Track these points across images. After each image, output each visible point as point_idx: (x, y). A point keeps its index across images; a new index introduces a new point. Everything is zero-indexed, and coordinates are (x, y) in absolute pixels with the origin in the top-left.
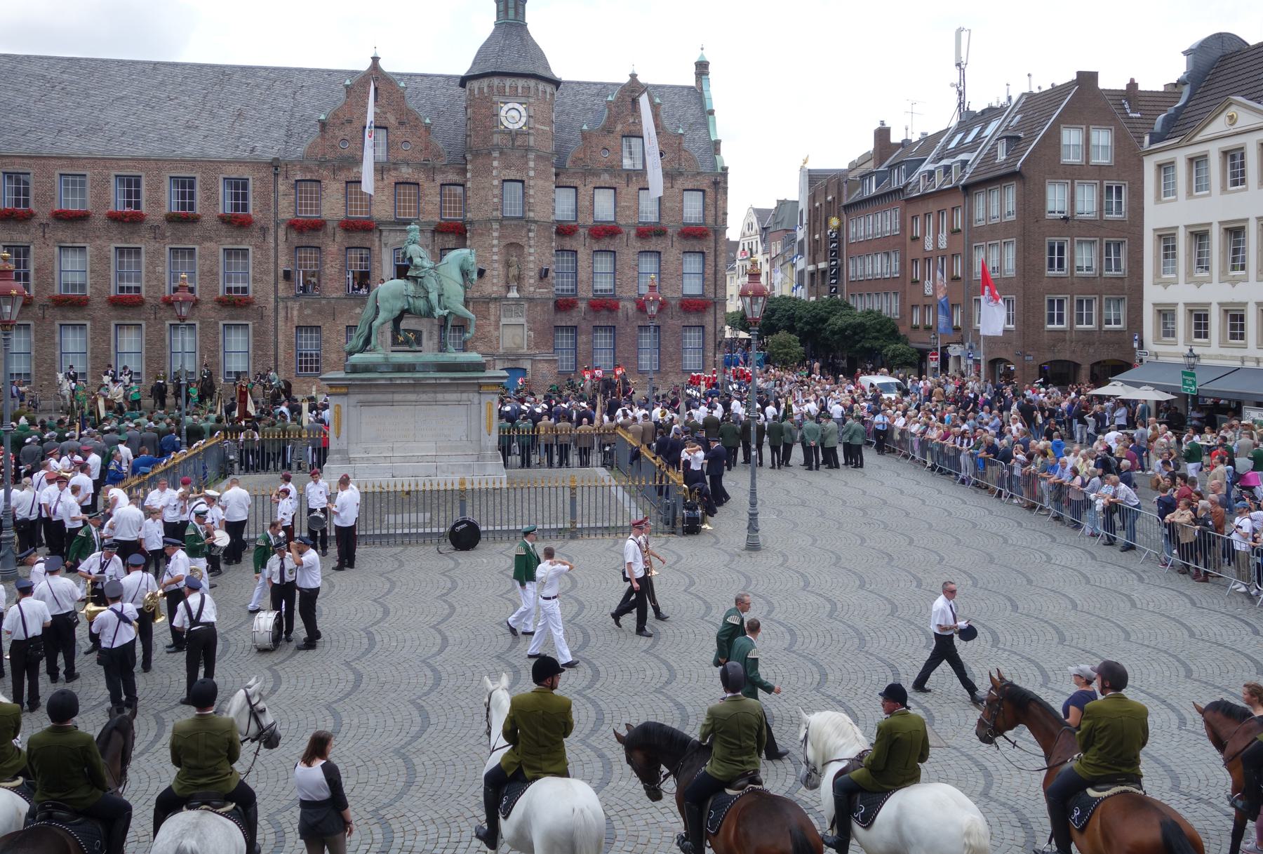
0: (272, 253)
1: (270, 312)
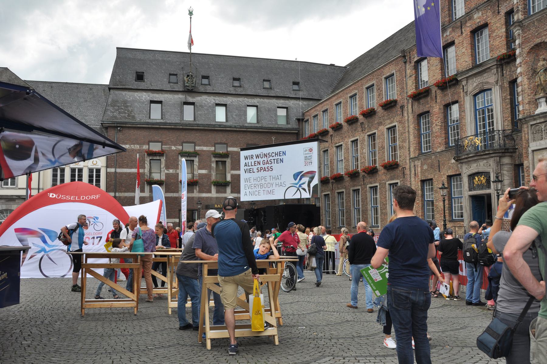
0: (407, 125)
1: (407, 172)
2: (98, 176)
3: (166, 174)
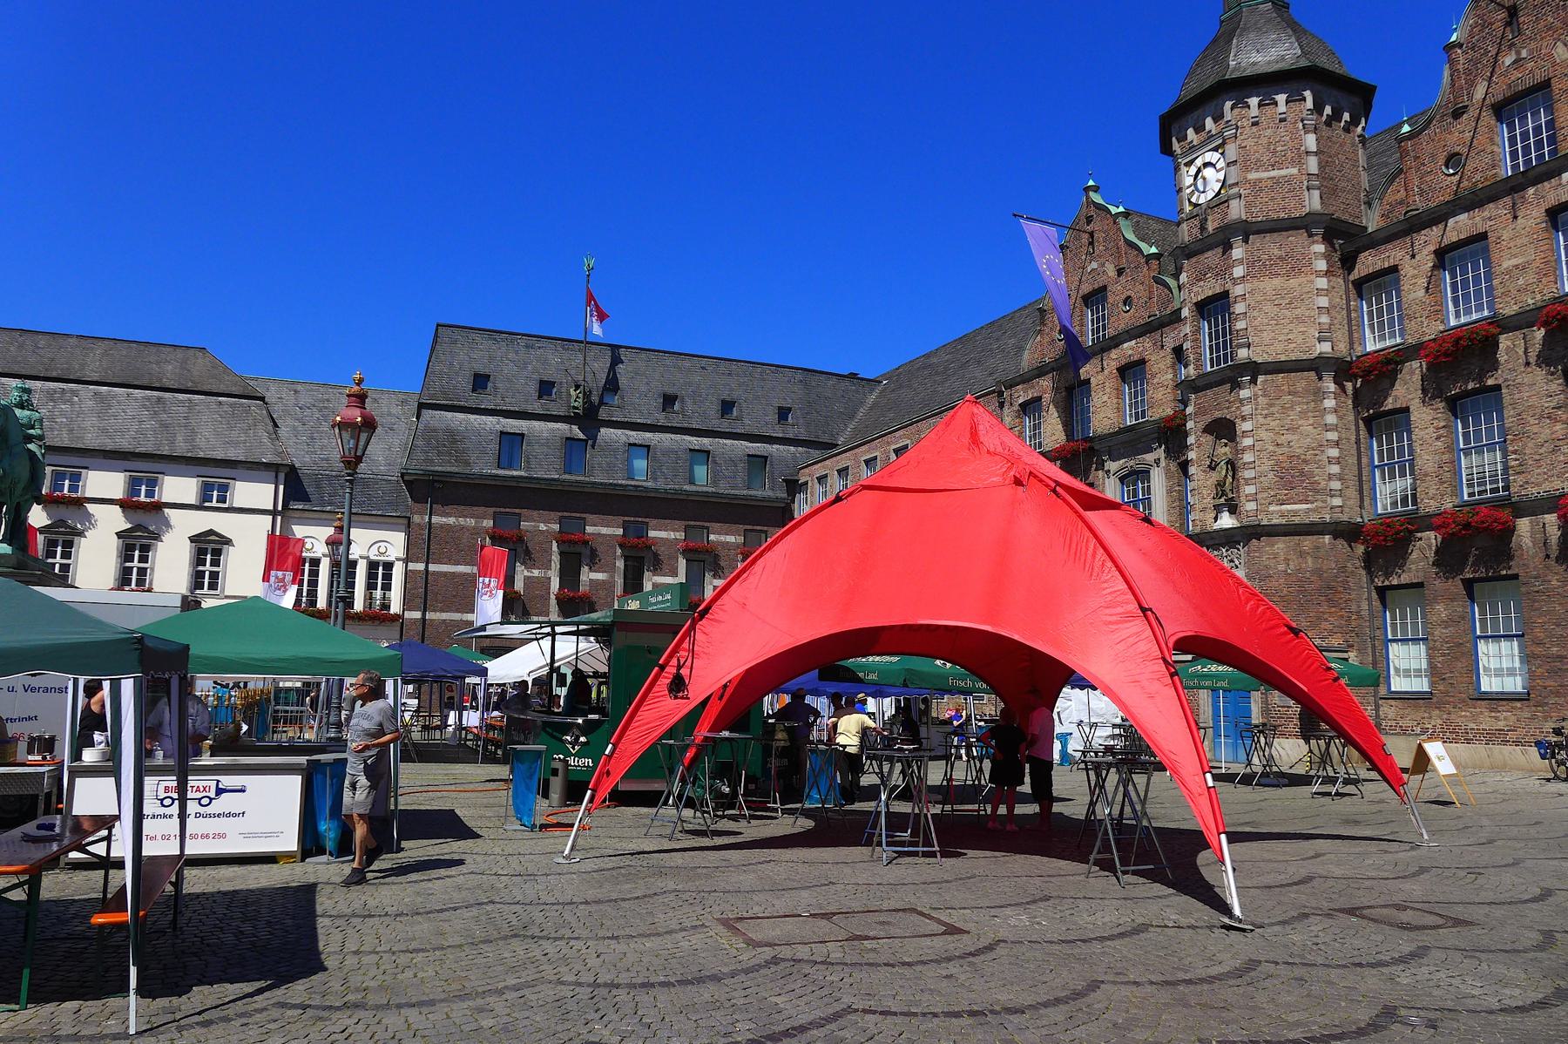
2: (388, 577)
3: (526, 578)
